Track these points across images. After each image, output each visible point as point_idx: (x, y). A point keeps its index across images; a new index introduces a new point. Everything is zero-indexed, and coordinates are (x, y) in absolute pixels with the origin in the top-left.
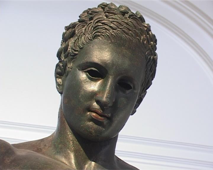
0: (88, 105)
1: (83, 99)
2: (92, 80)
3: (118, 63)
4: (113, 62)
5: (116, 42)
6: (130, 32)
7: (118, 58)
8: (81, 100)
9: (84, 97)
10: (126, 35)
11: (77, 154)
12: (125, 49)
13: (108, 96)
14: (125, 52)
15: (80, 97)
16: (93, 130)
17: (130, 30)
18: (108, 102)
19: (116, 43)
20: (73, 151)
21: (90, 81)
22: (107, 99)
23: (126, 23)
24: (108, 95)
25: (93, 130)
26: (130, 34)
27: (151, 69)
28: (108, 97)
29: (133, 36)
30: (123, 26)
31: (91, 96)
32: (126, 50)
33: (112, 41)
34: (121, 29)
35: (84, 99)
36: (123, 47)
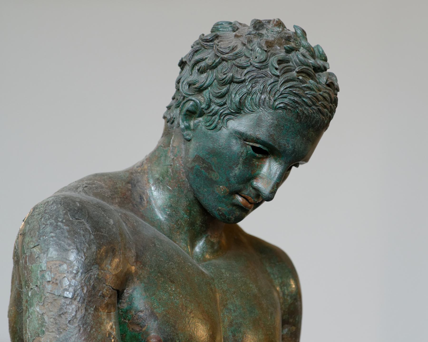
0: (239, 188)
1: (235, 180)
4: (295, 148)
5: (306, 123)
8: (232, 179)
9: (237, 178)
15: (231, 175)
16: (234, 217)
19: (305, 124)
25: (234, 217)
26: (325, 114)
30: (319, 101)
31: (248, 178)
32: (313, 132)
33: (301, 121)
34: (317, 106)
35: (236, 180)
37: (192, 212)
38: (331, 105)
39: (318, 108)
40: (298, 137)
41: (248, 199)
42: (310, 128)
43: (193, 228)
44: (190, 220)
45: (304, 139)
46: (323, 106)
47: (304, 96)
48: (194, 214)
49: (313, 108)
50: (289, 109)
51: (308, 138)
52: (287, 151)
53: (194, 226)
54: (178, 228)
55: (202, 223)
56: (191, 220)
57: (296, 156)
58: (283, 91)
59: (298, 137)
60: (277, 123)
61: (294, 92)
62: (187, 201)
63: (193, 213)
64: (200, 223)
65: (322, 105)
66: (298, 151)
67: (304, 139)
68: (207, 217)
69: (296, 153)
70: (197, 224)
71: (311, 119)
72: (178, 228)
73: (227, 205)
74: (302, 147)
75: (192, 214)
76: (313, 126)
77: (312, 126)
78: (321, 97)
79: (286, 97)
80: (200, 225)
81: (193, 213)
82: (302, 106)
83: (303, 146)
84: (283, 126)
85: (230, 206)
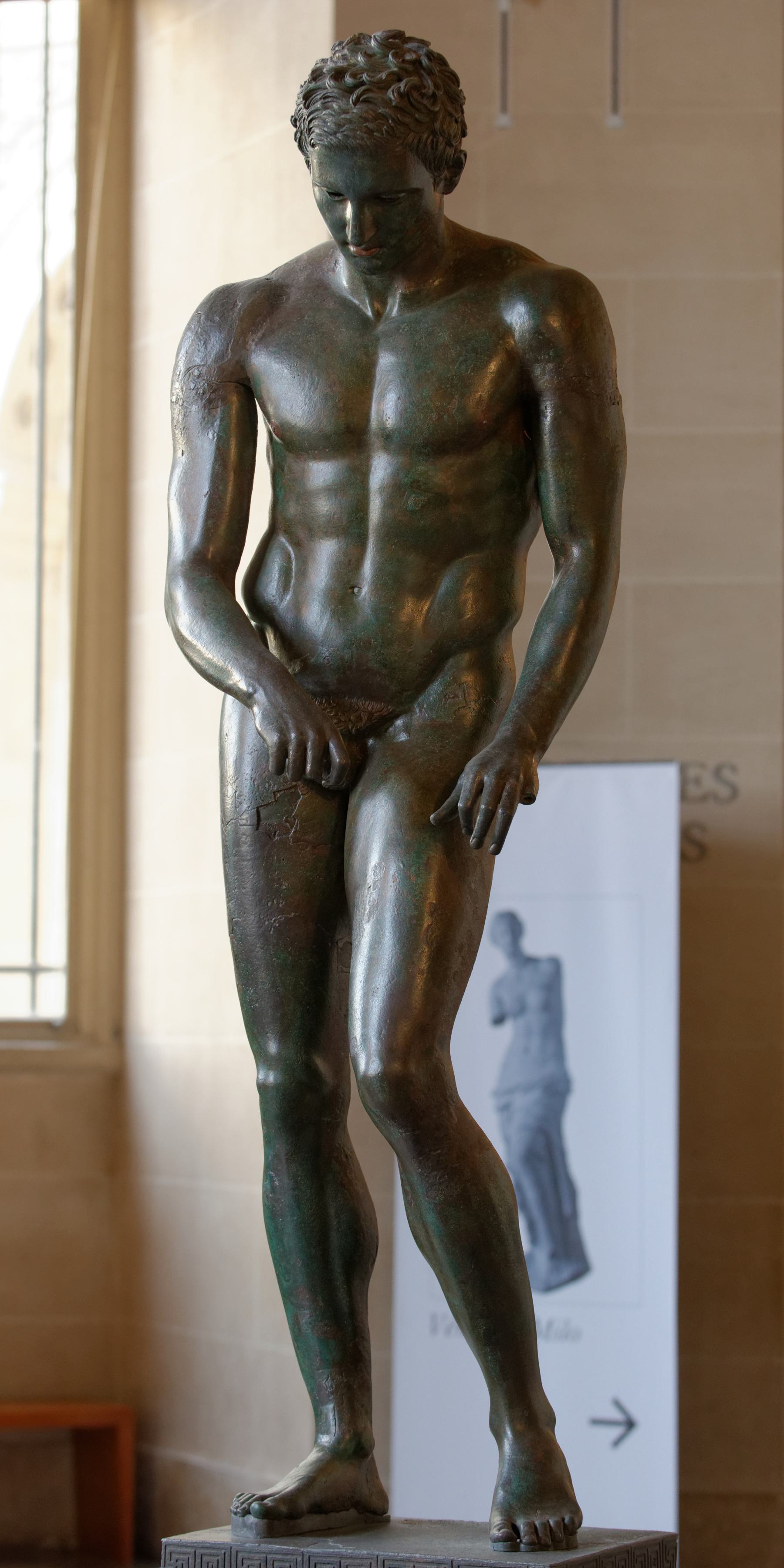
13: (356, 233)
14: (360, 164)
22: (355, 239)
24: (354, 232)
70: (375, 279)
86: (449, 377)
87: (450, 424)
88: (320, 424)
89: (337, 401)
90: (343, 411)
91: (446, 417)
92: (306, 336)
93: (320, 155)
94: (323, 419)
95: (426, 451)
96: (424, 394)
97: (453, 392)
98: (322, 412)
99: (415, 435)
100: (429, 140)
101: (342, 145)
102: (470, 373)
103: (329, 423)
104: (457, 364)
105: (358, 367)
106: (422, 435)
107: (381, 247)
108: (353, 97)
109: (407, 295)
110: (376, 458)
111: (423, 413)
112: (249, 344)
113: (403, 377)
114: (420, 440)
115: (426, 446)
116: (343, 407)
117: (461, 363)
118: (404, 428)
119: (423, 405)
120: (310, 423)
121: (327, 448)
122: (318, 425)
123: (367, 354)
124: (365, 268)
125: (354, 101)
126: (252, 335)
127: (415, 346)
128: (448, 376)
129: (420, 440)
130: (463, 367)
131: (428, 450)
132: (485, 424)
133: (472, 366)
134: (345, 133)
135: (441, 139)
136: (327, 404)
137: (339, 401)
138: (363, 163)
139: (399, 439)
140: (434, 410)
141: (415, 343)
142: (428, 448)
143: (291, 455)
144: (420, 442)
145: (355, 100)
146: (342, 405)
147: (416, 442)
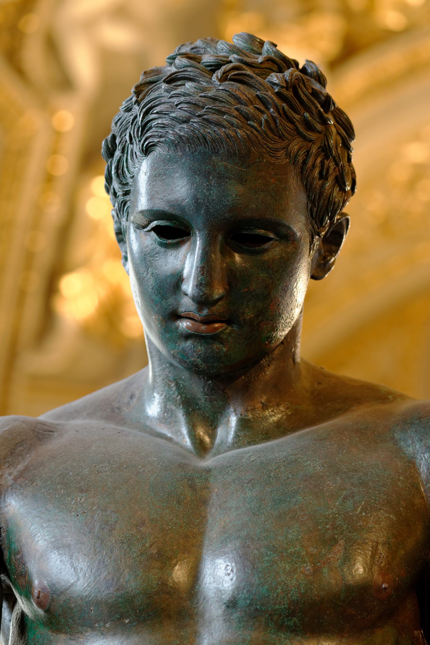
1: (157, 295)
2: (166, 246)
3: (210, 198)
4: (198, 199)
6: (225, 117)
7: (207, 185)
10: (215, 129)
11: (190, 410)
12: (222, 160)
13: (201, 280)
14: (222, 168)
16: (198, 358)
17: (224, 113)
18: (203, 295)
20: (180, 405)
21: (163, 250)
22: (200, 289)
23: (210, 98)
24: (200, 278)
25: (198, 358)
26: (225, 123)
27: (321, 173)
28: (201, 284)
29: (232, 125)
30: (203, 108)
32: (224, 161)
34: (199, 116)
35: (159, 295)
36: (216, 156)
37: (180, 382)
38: (239, 106)
39: (204, 119)
40: (196, 179)
41: (191, 317)
42: (210, 156)
43: (197, 407)
44: (181, 396)
45: (211, 178)
46: (214, 111)
47: (171, 112)
48: (185, 384)
49: (192, 122)
50: (158, 142)
51: (219, 174)
52: (186, 210)
53: (197, 404)
54: (169, 417)
55: (207, 395)
56: (184, 395)
57: (208, 211)
58: (144, 120)
59: (196, 179)
60: (155, 173)
61: (155, 112)
62: (165, 369)
63: (182, 382)
64: (205, 395)
65: (210, 112)
66: (208, 201)
67: (211, 178)
68: (210, 382)
69: (207, 206)
71: (199, 140)
72: (169, 417)
73: (176, 343)
74: (213, 193)
75: (181, 385)
76: (215, 152)
77: (212, 152)
78: (203, 99)
79: (151, 128)
80: (206, 398)
81: (182, 382)
82: (173, 127)
83: (215, 191)
84: (164, 174)
85: (180, 341)
86: (329, 515)
87: (333, 581)
88: (118, 579)
89: (147, 545)
90: (157, 560)
91: (326, 572)
92: (95, 466)
93: (153, 168)
94: (124, 570)
95: (291, 623)
96: (290, 536)
97: (336, 536)
98: (123, 561)
99: (275, 595)
100: (319, 160)
101: (198, 138)
102: (361, 512)
103: (133, 577)
104: (340, 499)
105: (179, 502)
106: (287, 595)
107: (229, 322)
108: (217, 73)
109: (249, 420)
110: (206, 636)
111: (289, 563)
112: (3, 477)
113: (254, 514)
114: (284, 605)
115: (292, 614)
116: (156, 554)
117: (345, 498)
118: (259, 585)
119: (289, 551)
120: (102, 576)
121: (127, 618)
122: (115, 579)
123: (193, 487)
124: (200, 356)
125: (219, 78)
126: (9, 467)
127: (270, 477)
128: (327, 513)
129: (284, 605)
130: (349, 503)
131: (295, 622)
132: (385, 589)
133: (363, 503)
134: (205, 117)
135: (332, 165)
136: (131, 549)
137: (151, 546)
138: (225, 167)
139: (248, 602)
140: (306, 559)
141: (270, 474)
142: (295, 619)
143: (62, 637)
144: (283, 607)
145: (222, 77)
146: (155, 552)
147: (277, 607)
